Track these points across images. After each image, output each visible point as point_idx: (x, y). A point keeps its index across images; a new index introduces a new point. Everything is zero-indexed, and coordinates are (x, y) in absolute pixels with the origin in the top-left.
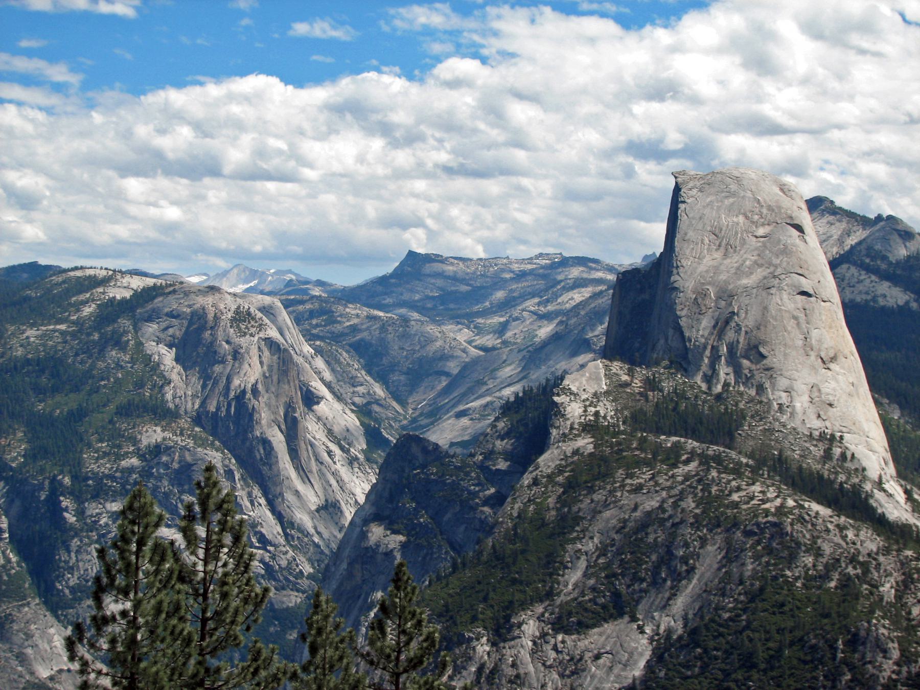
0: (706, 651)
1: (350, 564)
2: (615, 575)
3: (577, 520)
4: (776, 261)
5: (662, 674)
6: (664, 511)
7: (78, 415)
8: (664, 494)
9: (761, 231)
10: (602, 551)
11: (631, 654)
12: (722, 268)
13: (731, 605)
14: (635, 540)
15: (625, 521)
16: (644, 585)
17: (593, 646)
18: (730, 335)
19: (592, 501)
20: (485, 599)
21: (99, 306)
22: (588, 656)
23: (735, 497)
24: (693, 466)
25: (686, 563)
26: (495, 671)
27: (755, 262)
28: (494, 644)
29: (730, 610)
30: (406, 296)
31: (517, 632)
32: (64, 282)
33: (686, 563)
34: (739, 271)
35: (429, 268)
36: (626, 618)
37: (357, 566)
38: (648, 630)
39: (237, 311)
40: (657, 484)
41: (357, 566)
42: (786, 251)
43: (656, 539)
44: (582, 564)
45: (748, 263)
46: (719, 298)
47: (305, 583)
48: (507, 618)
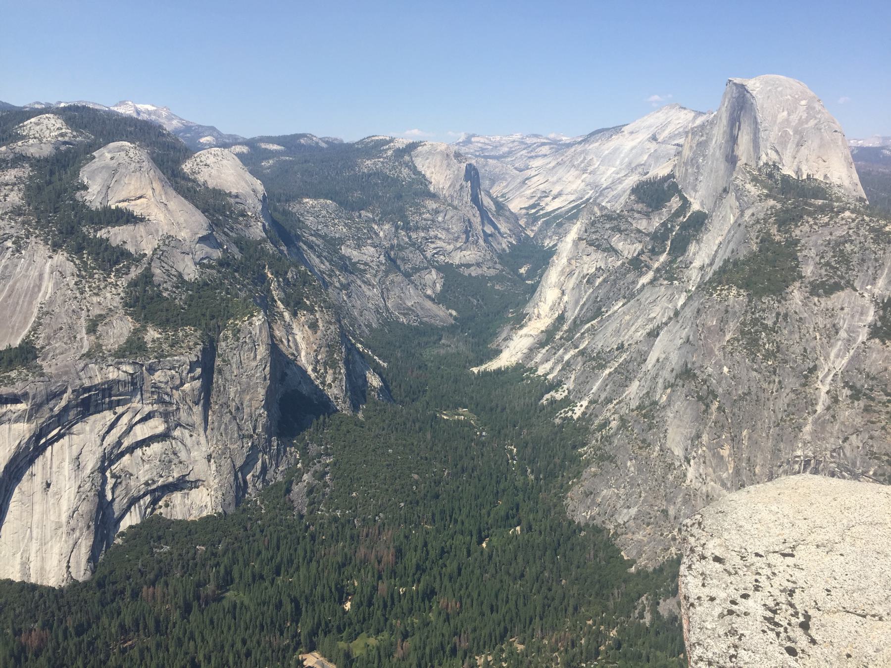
1: (569, 261)
2: (837, 268)
3: (799, 241)
6: (850, 236)
7: (399, 197)
8: (846, 227)
12: (790, 120)
14: (840, 249)
16: (854, 273)
17: (836, 304)
18: (804, 151)
19: (801, 231)
20: (769, 280)
21: (394, 151)
22: (835, 309)
24: (847, 214)
26: (786, 316)
28: (779, 302)
30: (467, 150)
31: (791, 296)
32: (372, 141)
34: (801, 122)
35: (473, 139)
37: (573, 262)
38: (866, 295)
39: (455, 153)
40: (835, 223)
41: (573, 262)
43: (852, 250)
45: (803, 117)
46: (794, 134)
47: (498, 266)
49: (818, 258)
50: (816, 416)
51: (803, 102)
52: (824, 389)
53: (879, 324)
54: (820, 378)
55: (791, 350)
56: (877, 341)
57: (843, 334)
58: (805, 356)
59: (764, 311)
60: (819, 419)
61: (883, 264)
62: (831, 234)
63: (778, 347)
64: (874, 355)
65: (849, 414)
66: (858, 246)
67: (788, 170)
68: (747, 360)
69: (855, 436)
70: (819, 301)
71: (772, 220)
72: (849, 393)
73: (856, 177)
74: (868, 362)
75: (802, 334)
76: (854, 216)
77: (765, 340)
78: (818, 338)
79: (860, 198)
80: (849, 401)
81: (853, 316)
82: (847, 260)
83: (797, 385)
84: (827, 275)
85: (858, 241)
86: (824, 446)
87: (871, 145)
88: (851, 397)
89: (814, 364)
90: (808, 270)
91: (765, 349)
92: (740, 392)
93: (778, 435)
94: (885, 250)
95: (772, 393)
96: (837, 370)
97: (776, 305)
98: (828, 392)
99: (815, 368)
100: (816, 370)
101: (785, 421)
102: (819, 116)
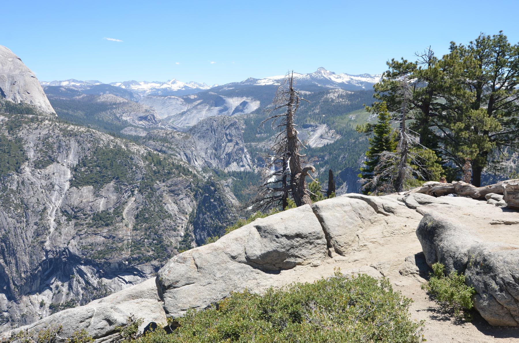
0: (89, 167)
2: (46, 152)
3: (22, 139)
4: (21, 68)
5: (80, 175)
6: (51, 134)
8: (47, 129)
9: (10, 59)
10: (37, 145)
11: (64, 171)
13: (90, 155)
15: (39, 137)
16: (57, 154)
18: (16, 88)
19: (23, 133)
20: (8, 163)
22: (50, 174)
23: (69, 129)
25: (67, 146)
26: (23, 183)
27: (14, 68)
28: (18, 175)
29: (90, 156)
31: (24, 171)
33: (67, 146)
36: (55, 163)
38: (65, 164)
40: (41, 127)
42: (21, 65)
43: (53, 141)
44: (32, 150)
48: (19, 168)
49: (35, 147)
50: (51, 235)
51: (10, 59)
52: (52, 219)
53: (74, 179)
54: (49, 214)
55: (30, 201)
56: (75, 187)
57: (56, 187)
58: (38, 203)
59: (9, 182)
60: (53, 236)
61: (70, 148)
62: (40, 134)
63: (22, 201)
64: (75, 195)
65: (69, 229)
66: (56, 139)
67: (9, 99)
68: (4, 212)
69: (73, 240)
70: (40, 171)
71: (4, 128)
72: (66, 218)
73: (48, 102)
74: (72, 200)
75: (34, 191)
76: (50, 123)
77: (13, 198)
78: (44, 191)
79: (52, 113)
80: (66, 223)
81: (60, 176)
82: (51, 147)
83: (37, 220)
84: (42, 156)
85: (55, 137)
86: (58, 250)
87: (54, 85)
88: (67, 220)
89: (44, 206)
90: (31, 154)
91: (14, 204)
92: (4, 232)
93: (32, 251)
94: (69, 140)
95: (23, 228)
96: (57, 207)
97: (16, 177)
98: (55, 220)
99: (45, 209)
100: (45, 210)
101: (34, 243)
102: (21, 68)
